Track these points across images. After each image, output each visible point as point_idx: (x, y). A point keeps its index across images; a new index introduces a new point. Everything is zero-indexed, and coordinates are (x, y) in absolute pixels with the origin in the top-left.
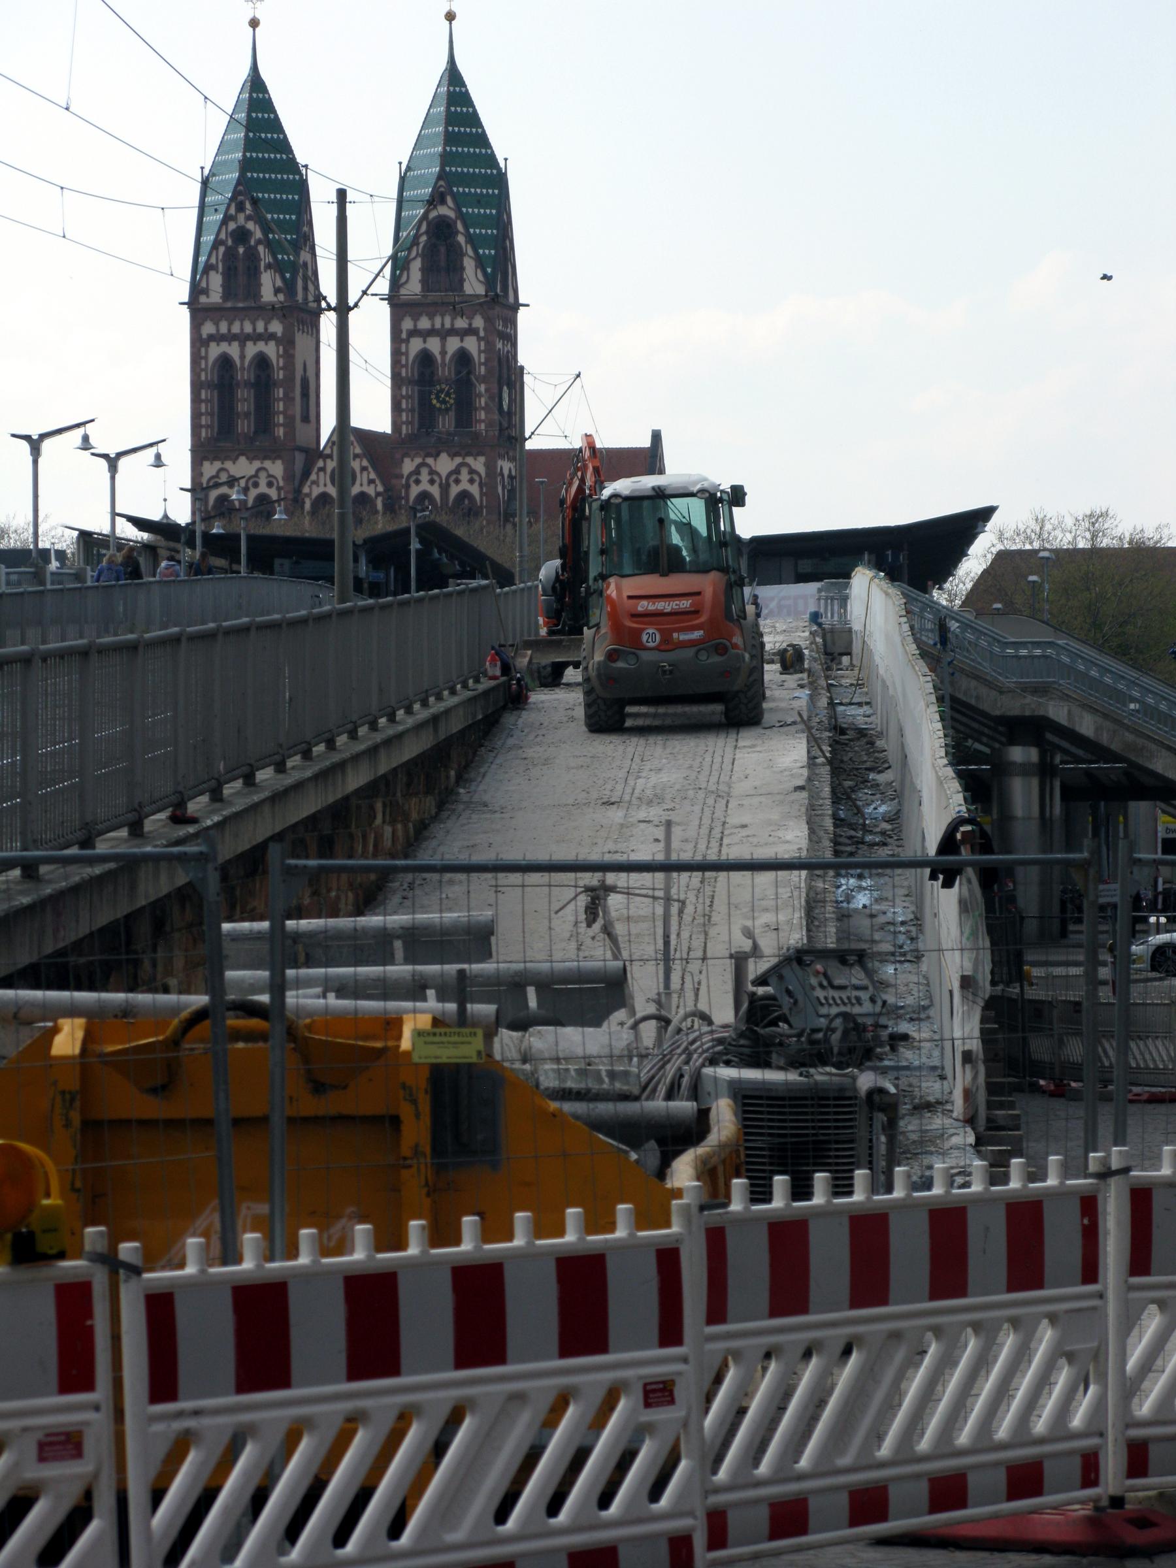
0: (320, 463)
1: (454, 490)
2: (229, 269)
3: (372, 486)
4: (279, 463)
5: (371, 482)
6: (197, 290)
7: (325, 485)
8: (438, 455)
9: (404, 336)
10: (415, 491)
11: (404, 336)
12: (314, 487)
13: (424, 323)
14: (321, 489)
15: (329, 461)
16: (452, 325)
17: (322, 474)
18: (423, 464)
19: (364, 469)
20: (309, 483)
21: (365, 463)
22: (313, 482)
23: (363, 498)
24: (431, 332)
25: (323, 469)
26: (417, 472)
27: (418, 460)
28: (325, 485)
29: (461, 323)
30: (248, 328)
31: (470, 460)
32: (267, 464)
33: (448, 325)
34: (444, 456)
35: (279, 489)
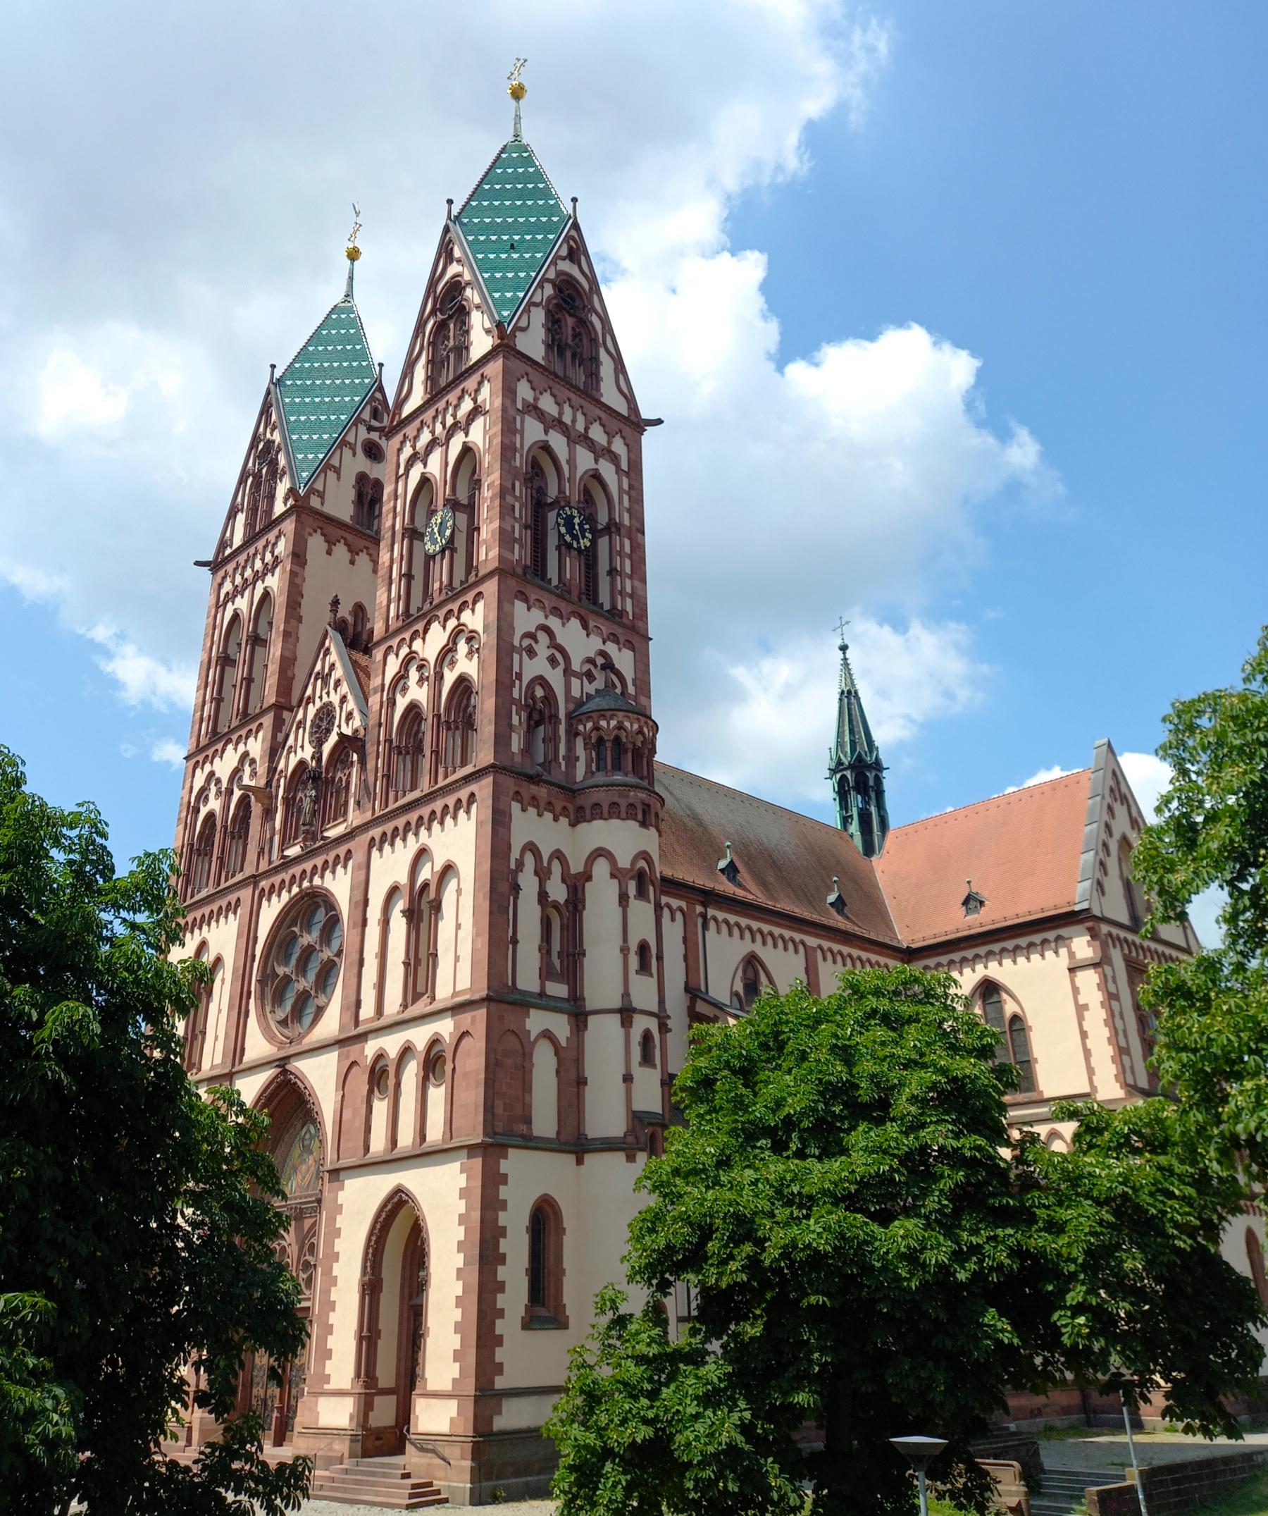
0: (300, 716)
6: (223, 544)
8: (426, 631)
9: (401, 471)
11: (401, 471)
13: (426, 437)
16: (454, 416)
19: (343, 699)
21: (344, 688)
24: (433, 444)
26: (401, 677)
27: (404, 651)
28: (302, 747)
29: (467, 405)
31: (466, 617)
33: (450, 421)
34: (435, 627)
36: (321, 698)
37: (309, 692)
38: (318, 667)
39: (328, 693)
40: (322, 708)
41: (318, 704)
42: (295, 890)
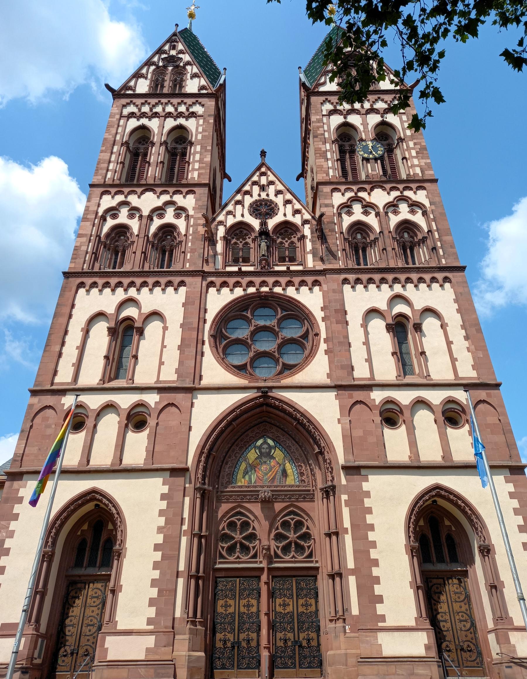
1: (394, 220)
2: (157, 80)
3: (298, 216)
4: (190, 197)
5: (296, 212)
7: (243, 215)
10: (347, 221)
12: (230, 217)
14: (239, 218)
15: (247, 197)
17: (239, 207)
18: (356, 199)
20: (224, 212)
22: (229, 213)
23: (286, 228)
25: (238, 202)
28: (243, 215)
30: (170, 109)
32: (178, 198)
35: (187, 217)
36: (259, 195)
37: (247, 188)
38: (255, 178)
39: (268, 195)
40: (260, 200)
41: (256, 197)
42: (252, 290)
